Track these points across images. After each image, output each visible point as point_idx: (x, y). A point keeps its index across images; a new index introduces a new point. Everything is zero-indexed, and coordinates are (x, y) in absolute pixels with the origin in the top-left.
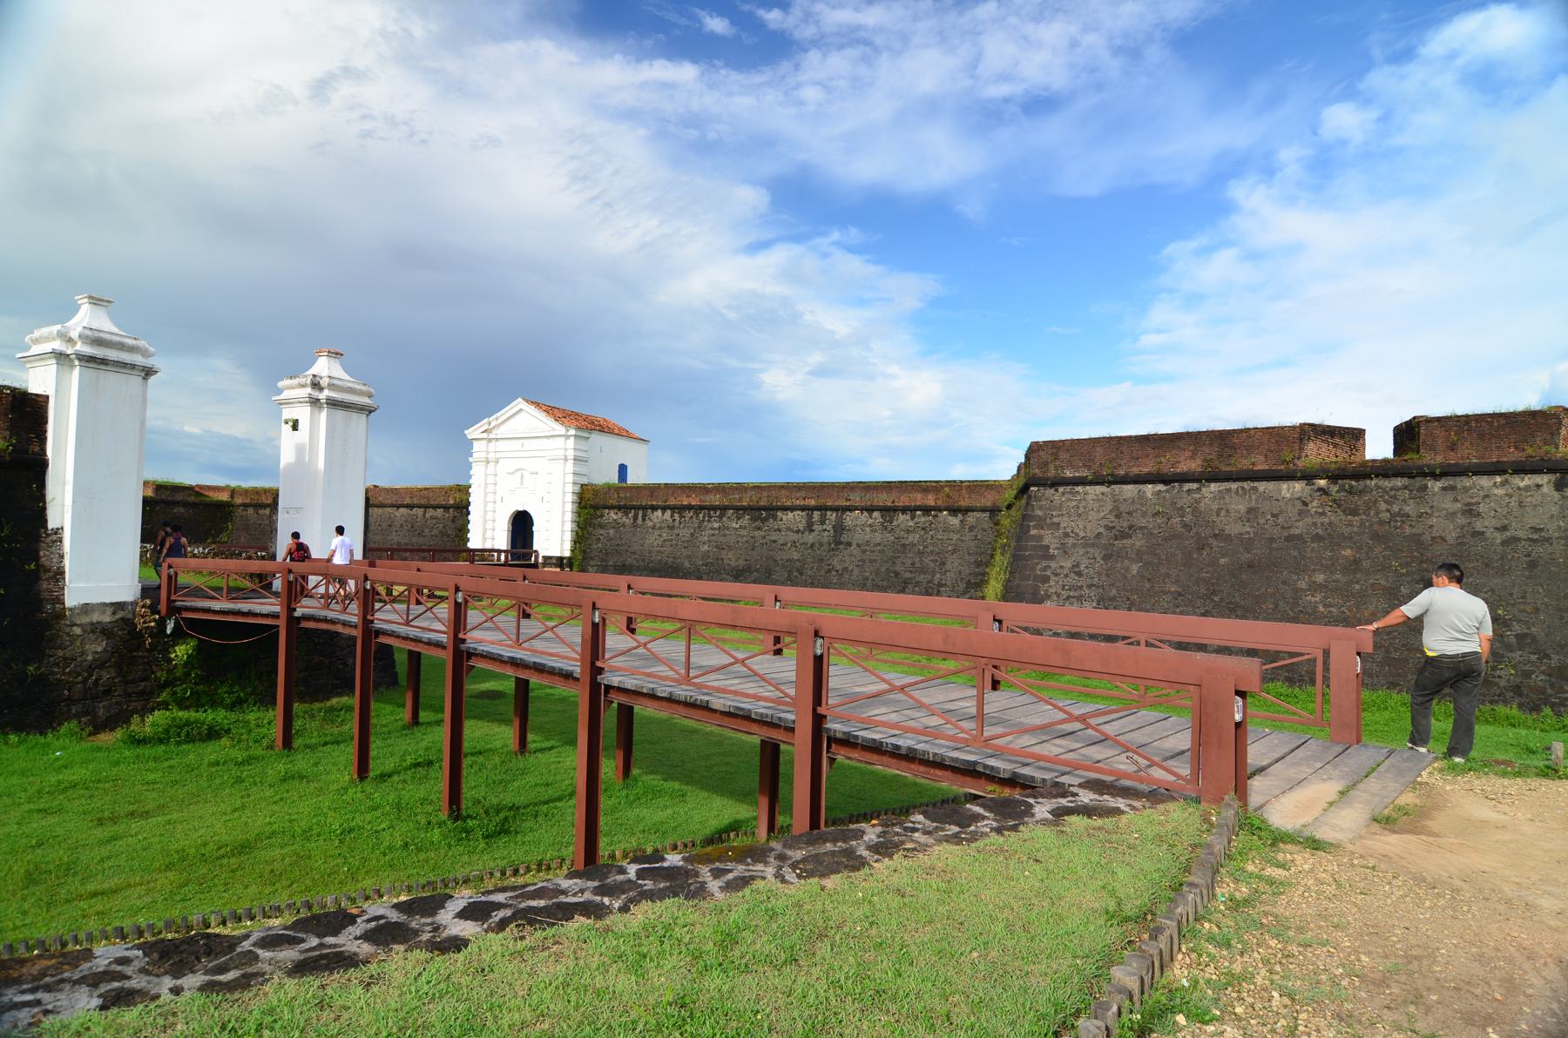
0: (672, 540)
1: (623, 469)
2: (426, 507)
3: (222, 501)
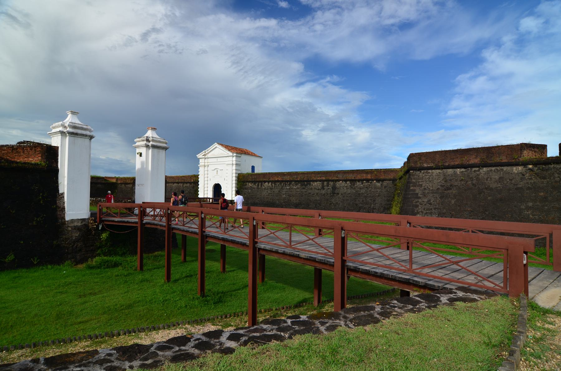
1: (253, 168)
2: (183, 183)
3: (113, 182)
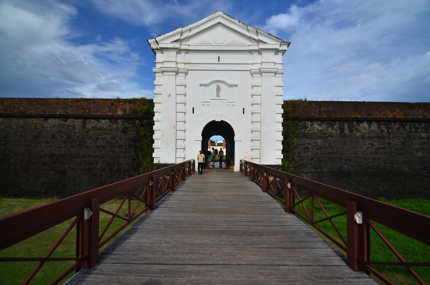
0: (385, 148)
2: (85, 118)
